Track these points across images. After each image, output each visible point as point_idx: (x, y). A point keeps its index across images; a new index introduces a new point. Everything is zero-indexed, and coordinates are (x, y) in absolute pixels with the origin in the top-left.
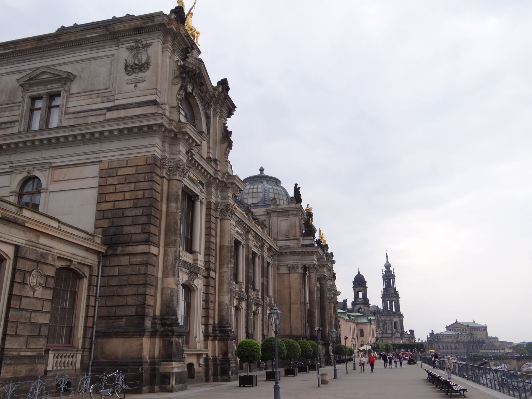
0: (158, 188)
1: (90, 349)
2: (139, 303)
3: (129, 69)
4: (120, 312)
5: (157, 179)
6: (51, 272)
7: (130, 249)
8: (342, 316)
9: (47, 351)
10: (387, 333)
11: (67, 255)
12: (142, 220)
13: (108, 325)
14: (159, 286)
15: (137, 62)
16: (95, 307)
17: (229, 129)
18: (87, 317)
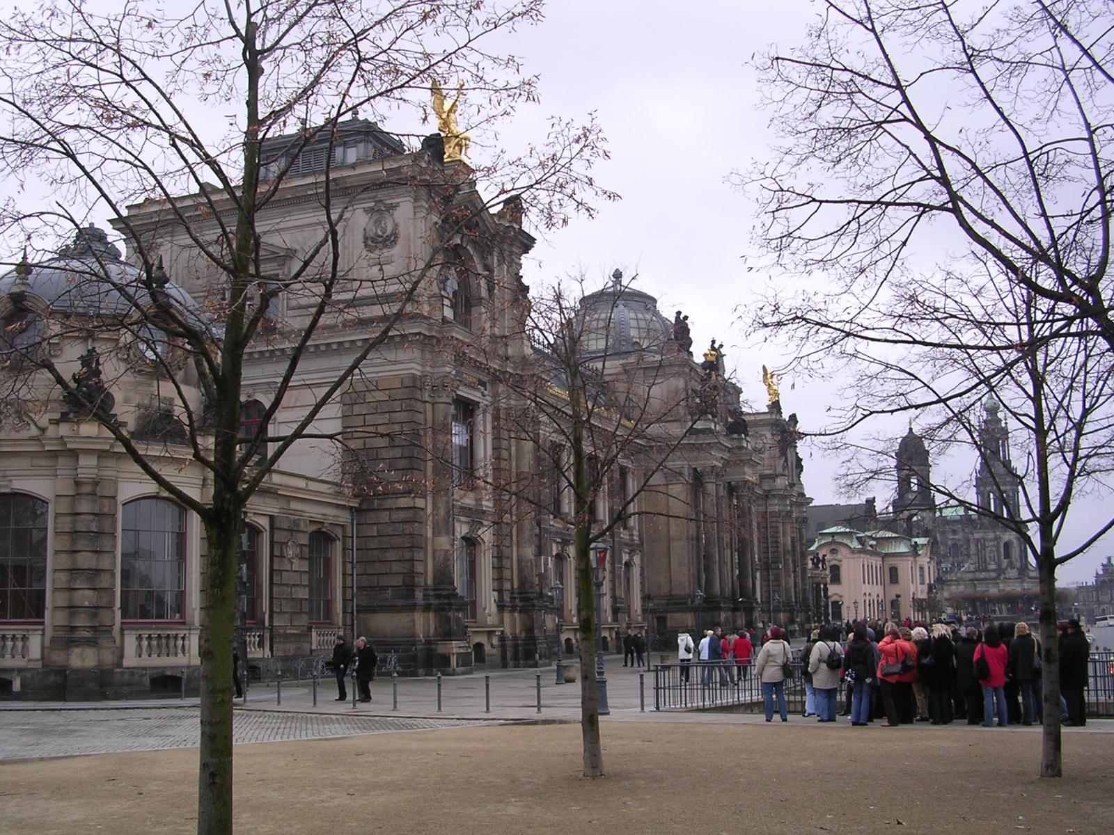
0: (420, 418)
1: (352, 625)
2: (406, 571)
3: (369, 242)
4: (384, 581)
5: (419, 406)
6: (304, 539)
7: (389, 503)
8: (845, 541)
9: (310, 629)
10: (986, 570)
11: (319, 517)
12: (402, 464)
13: (370, 599)
14: (430, 548)
15: (380, 233)
16: (352, 575)
17: (525, 281)
18: (344, 588)
